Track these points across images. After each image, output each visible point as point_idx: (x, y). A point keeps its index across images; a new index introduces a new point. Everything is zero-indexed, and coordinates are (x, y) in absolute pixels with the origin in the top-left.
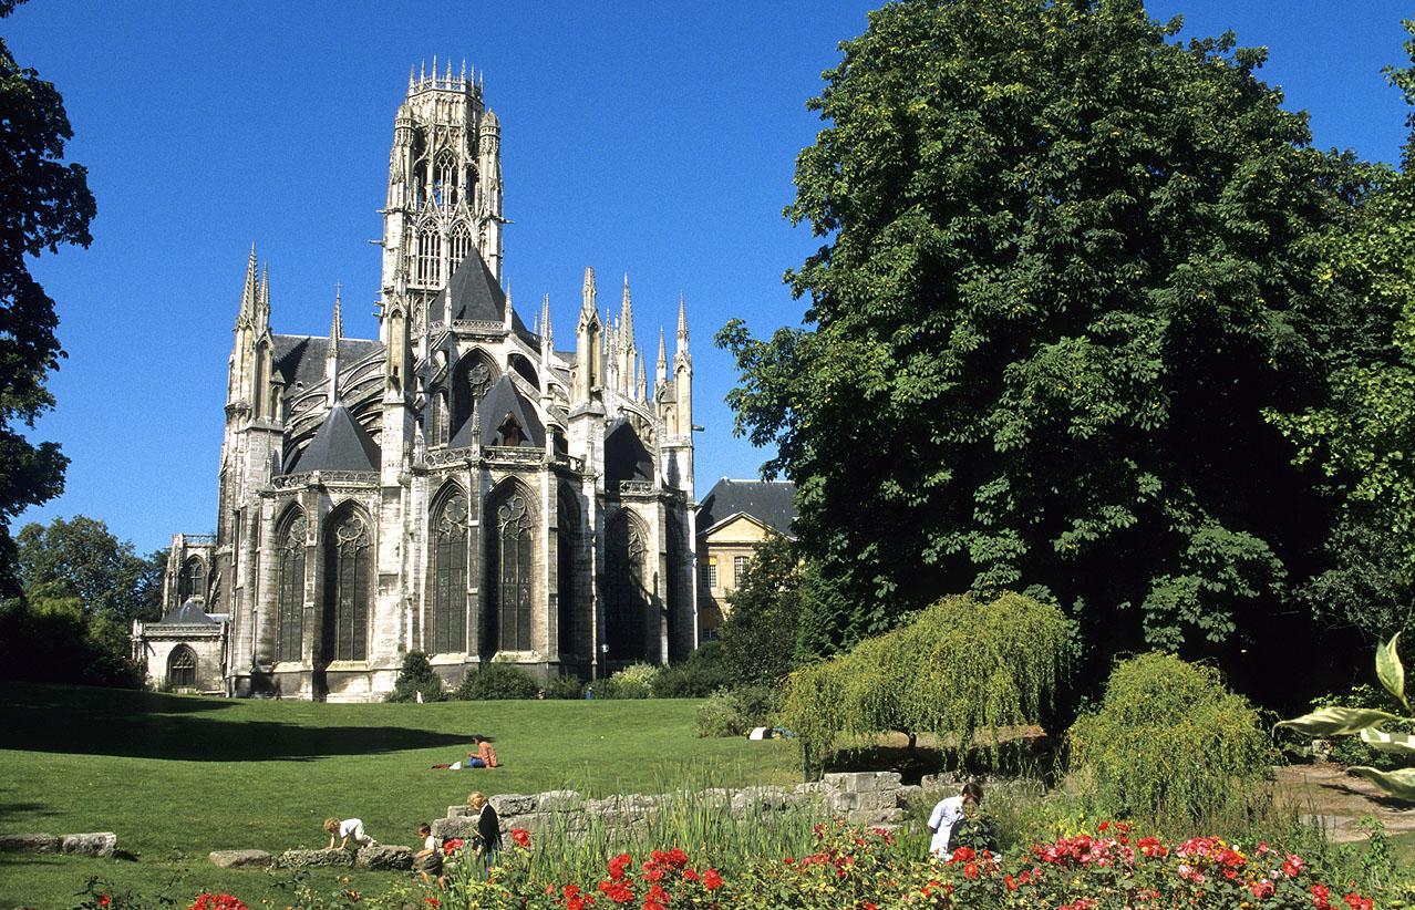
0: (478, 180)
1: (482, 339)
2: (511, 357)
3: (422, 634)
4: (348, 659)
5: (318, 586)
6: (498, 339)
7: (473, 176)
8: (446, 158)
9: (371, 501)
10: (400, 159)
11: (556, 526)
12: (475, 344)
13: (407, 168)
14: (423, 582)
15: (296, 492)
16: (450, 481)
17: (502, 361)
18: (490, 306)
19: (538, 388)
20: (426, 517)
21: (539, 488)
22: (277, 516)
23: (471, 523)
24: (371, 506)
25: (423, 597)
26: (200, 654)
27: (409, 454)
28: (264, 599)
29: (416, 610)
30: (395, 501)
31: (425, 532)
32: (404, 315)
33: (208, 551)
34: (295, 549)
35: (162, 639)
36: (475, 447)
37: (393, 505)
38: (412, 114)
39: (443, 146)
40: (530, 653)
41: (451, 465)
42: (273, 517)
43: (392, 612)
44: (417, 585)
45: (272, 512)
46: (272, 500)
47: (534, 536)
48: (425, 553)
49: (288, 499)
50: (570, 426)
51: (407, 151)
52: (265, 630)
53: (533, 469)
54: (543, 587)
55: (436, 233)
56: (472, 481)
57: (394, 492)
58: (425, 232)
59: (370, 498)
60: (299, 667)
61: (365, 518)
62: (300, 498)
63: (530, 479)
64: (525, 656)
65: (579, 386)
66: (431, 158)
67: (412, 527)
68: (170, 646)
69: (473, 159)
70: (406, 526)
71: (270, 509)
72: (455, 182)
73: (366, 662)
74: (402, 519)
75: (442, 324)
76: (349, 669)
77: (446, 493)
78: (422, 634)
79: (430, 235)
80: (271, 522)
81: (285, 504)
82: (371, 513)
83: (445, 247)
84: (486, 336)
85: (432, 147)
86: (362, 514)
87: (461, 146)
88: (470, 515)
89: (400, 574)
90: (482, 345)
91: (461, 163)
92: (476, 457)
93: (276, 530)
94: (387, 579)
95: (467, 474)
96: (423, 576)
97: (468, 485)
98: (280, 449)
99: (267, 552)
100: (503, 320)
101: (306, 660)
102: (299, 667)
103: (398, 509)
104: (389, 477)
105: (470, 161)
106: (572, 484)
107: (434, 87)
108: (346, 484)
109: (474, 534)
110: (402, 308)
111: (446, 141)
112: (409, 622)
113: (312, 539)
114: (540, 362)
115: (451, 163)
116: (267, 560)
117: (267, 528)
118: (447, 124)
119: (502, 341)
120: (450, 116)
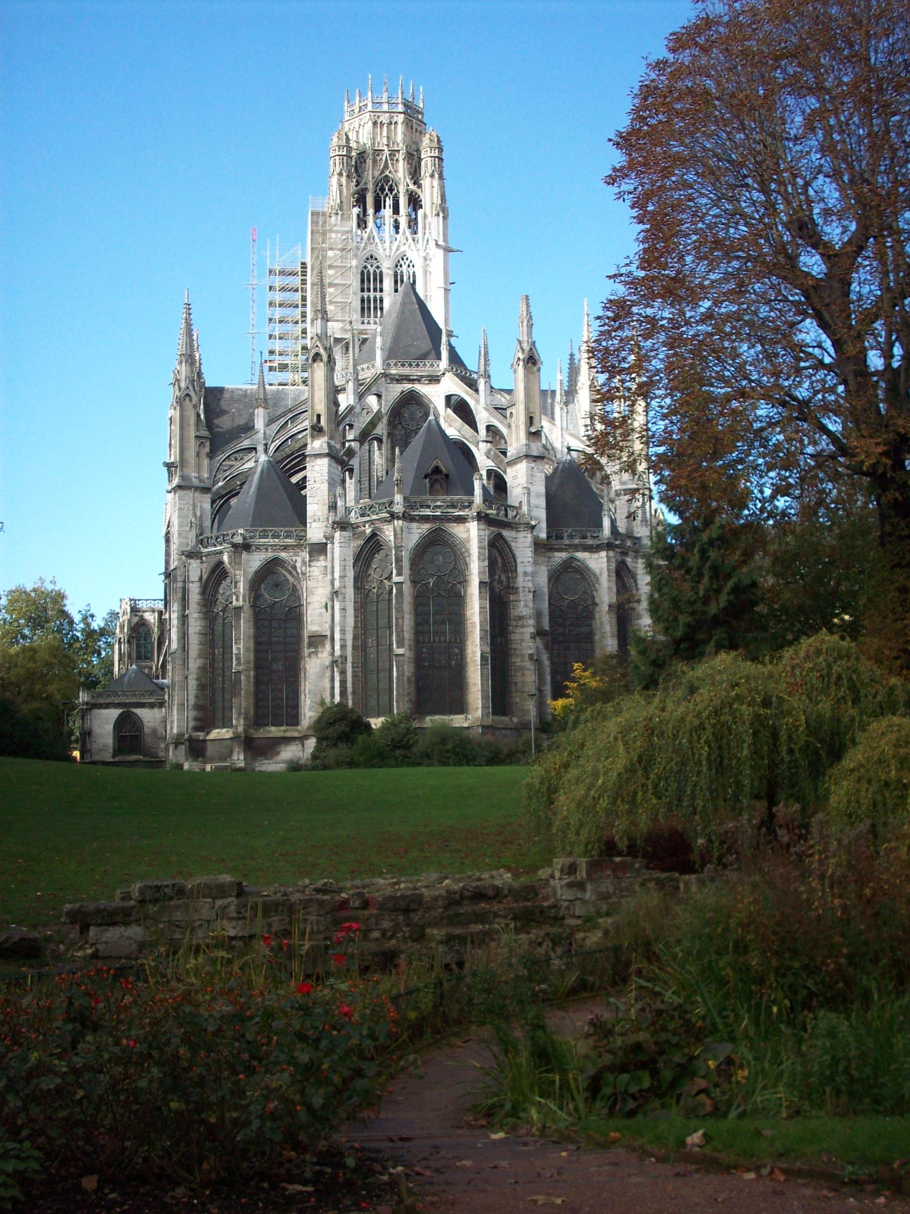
0: (421, 207)
1: (419, 380)
2: (448, 398)
3: (350, 697)
4: (281, 725)
5: (247, 649)
6: (434, 379)
7: (415, 202)
8: (385, 186)
9: (299, 559)
11: (487, 580)
12: (410, 386)
14: (349, 643)
15: (221, 552)
16: (374, 535)
17: (439, 403)
18: (426, 344)
19: (475, 429)
20: (351, 574)
21: (468, 540)
22: (205, 577)
23: (396, 579)
24: (298, 565)
25: (350, 659)
26: (145, 721)
27: (333, 507)
28: (194, 664)
29: (343, 672)
30: (322, 558)
31: (350, 591)
32: (325, 358)
33: (156, 615)
34: (224, 610)
35: (107, 706)
36: (398, 498)
37: (321, 563)
38: (348, 139)
40: (463, 716)
41: (374, 517)
42: (201, 579)
43: (321, 676)
44: (343, 647)
47: (465, 591)
48: (351, 612)
49: (214, 560)
50: (508, 470)
51: (344, 180)
52: (197, 697)
53: (462, 520)
54: (475, 648)
55: (378, 267)
56: (395, 534)
57: (319, 549)
58: (365, 267)
62: (226, 558)
63: (458, 530)
64: (458, 721)
65: (517, 427)
66: (370, 186)
67: (337, 584)
68: (115, 713)
69: (415, 183)
70: (332, 582)
72: (396, 210)
74: (329, 577)
75: (373, 366)
76: (281, 734)
77: (371, 547)
78: (350, 697)
81: (212, 564)
83: (388, 284)
84: (422, 377)
85: (370, 175)
86: (290, 573)
87: (400, 172)
88: (394, 571)
89: (328, 633)
90: (418, 387)
91: (402, 189)
92: (398, 508)
94: (317, 640)
95: (391, 528)
96: (349, 637)
97: (392, 538)
98: (207, 506)
99: (196, 615)
100: (439, 357)
104: (315, 532)
105: (412, 187)
106: (506, 533)
108: (271, 541)
109: (400, 591)
110: (322, 351)
112: (337, 685)
113: (237, 600)
114: (477, 401)
115: (391, 190)
116: (195, 625)
117: (194, 590)
118: (385, 148)
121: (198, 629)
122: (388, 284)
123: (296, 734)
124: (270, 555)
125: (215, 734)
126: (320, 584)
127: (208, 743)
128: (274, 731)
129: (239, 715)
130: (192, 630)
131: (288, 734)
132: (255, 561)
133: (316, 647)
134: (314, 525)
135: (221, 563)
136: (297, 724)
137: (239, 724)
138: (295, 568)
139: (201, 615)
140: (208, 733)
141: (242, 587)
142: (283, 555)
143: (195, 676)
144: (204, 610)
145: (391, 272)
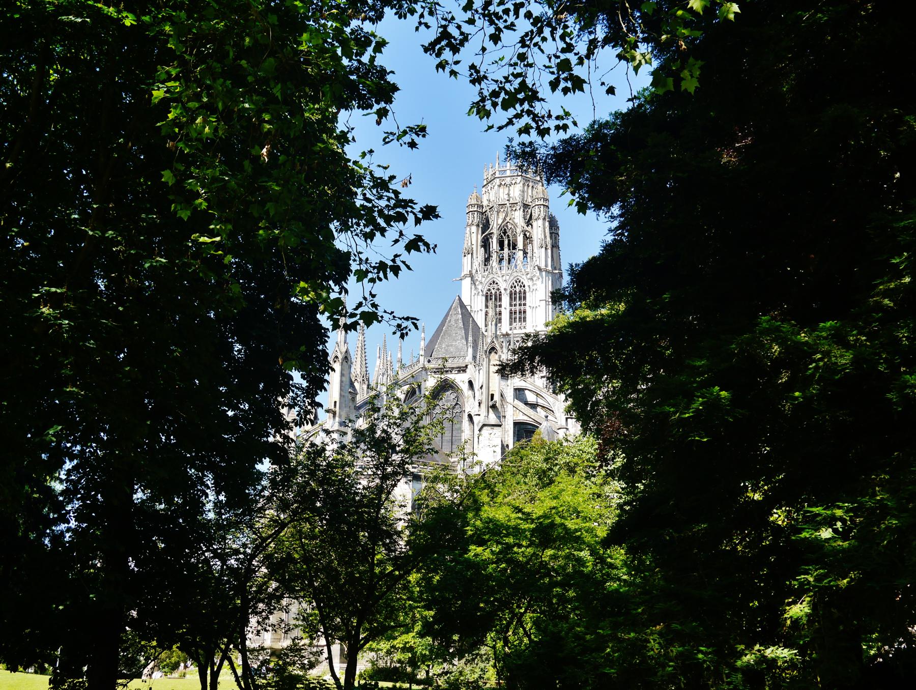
10: (474, 237)
13: (474, 242)
39: (505, 219)
55: (498, 289)
66: (495, 231)
79: (493, 292)
83: (506, 300)
84: (453, 368)
85: (496, 222)
107: (497, 175)
111: (506, 215)
118: (507, 202)
119: (464, 371)
120: (508, 195)
122: (506, 300)
145: (508, 292)
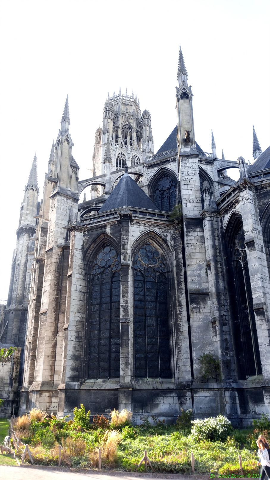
4: (157, 377)
9: (169, 235)
22: (86, 246)
24: (169, 239)
30: (198, 230)
34: (102, 273)
42: (83, 248)
45: (82, 244)
46: (82, 234)
57: (197, 222)
59: (168, 232)
60: (111, 384)
61: (163, 248)
62: (108, 230)
71: (78, 240)
73: (173, 380)
80: (81, 252)
81: (94, 236)
82: (169, 244)
86: (161, 246)
89: (213, 290)
93: (84, 258)
94: (197, 297)
99: (78, 276)
101: (124, 377)
102: (111, 384)
103: (203, 237)
113: (125, 259)
121: (78, 288)
123: (171, 386)
124: (146, 229)
125: (89, 384)
126: (198, 250)
127: (83, 393)
128: (149, 383)
129: (127, 364)
130: (74, 288)
131: (165, 386)
132: (135, 232)
133: (198, 303)
134: (189, 205)
135: (105, 233)
136: (169, 376)
137: (126, 374)
138: (165, 241)
139: (82, 277)
140: (82, 383)
141: (129, 250)
142: (157, 230)
143: (74, 328)
144: (84, 272)
